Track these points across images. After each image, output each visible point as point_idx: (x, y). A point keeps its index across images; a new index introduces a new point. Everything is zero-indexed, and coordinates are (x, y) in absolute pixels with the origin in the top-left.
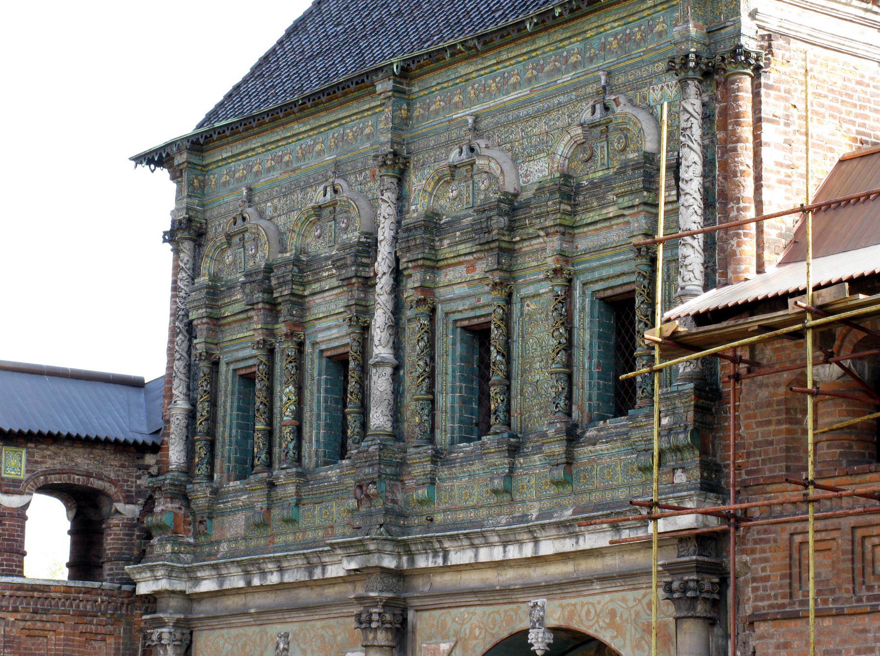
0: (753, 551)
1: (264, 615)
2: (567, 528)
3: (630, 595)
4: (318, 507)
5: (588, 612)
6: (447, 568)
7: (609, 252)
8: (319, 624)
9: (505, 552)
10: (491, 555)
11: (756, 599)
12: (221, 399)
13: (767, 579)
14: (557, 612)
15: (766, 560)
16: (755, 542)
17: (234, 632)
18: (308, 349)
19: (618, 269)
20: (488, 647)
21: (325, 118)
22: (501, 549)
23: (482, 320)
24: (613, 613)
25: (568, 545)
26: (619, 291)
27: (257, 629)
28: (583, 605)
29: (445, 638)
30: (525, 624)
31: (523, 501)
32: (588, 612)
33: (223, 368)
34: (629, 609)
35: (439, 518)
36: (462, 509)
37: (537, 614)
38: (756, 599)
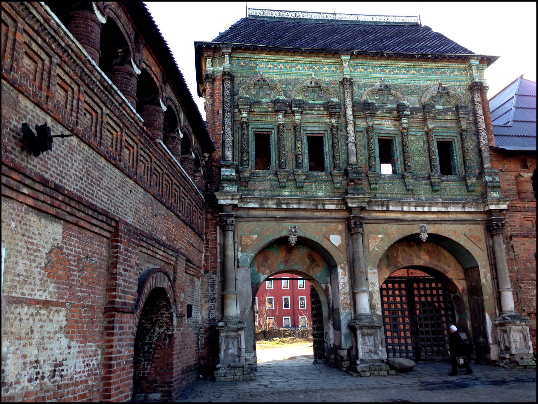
0: (509, 218)
3: (462, 226)
4: (314, 185)
5: (445, 230)
6: (388, 211)
7: (446, 129)
8: (312, 224)
9: (416, 209)
10: (409, 209)
11: (512, 231)
12: (250, 140)
13: (515, 226)
14: (432, 229)
15: (514, 221)
16: (510, 216)
17: (263, 224)
19: (449, 134)
20: (401, 237)
22: (414, 208)
23: (391, 138)
24: (455, 231)
25: (443, 209)
26: (445, 140)
27: (276, 224)
28: (442, 228)
30: (418, 231)
32: (445, 230)
33: (250, 129)
34: (461, 230)
35: (378, 195)
36: (390, 194)
38: (512, 231)
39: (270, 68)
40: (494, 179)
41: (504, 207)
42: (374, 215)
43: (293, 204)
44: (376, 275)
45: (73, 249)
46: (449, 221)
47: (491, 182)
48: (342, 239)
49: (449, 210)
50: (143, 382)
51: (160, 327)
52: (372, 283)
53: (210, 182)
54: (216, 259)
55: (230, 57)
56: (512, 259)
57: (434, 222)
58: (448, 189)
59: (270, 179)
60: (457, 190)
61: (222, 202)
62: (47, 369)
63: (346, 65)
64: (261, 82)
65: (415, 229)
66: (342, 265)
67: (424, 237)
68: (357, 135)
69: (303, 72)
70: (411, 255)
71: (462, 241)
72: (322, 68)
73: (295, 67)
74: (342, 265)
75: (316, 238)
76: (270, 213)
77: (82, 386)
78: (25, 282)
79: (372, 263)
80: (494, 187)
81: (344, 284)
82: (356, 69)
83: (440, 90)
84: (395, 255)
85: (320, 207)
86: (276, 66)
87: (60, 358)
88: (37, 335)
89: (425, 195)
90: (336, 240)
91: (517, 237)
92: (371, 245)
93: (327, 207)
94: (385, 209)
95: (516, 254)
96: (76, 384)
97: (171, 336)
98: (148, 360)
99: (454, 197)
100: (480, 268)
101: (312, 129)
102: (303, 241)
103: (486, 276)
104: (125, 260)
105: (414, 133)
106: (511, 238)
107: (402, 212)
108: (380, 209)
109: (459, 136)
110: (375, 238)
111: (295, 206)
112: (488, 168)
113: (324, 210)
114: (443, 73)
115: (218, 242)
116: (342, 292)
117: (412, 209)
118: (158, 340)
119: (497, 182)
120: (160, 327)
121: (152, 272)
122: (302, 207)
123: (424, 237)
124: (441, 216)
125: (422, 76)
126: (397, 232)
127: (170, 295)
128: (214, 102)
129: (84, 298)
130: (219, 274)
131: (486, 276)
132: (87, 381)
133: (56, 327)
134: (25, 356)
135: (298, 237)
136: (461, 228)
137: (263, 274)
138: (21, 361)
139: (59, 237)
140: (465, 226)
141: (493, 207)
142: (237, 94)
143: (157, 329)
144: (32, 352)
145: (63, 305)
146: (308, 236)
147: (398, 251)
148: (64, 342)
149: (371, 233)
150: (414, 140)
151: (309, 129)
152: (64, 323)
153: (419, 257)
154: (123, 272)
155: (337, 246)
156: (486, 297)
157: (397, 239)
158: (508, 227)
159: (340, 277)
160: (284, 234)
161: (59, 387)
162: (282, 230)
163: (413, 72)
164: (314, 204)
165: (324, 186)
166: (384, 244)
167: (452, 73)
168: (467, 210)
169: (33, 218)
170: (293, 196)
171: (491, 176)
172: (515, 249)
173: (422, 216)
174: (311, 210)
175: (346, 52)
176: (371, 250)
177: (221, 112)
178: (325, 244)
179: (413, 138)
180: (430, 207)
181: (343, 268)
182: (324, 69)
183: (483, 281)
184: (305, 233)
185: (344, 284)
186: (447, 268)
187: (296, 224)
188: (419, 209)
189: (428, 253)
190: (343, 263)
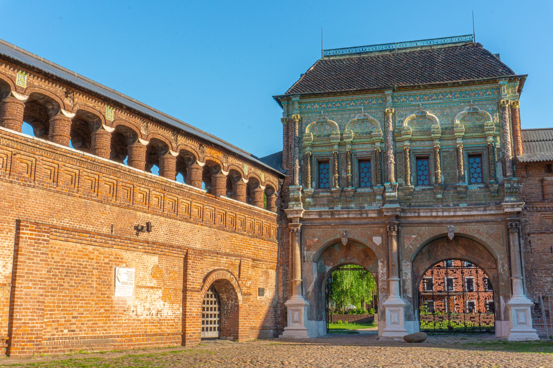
1: (337, 225)
2: (468, 209)
4: (361, 198)
5: (469, 230)
14: (458, 229)
18: (353, 157)
21: (361, 96)
24: (479, 230)
25: (466, 213)
29: (414, 235)
31: (447, 202)
32: (469, 230)
33: (313, 158)
37: (450, 229)
39: (330, 107)
40: (512, 186)
41: (519, 209)
42: (410, 219)
43: (344, 214)
44: (410, 267)
45: (164, 265)
46: (473, 222)
47: (509, 188)
48: (382, 239)
49: (472, 213)
50: (224, 330)
51: (232, 301)
52: (405, 273)
53: (283, 202)
54: (289, 256)
55: (300, 103)
56: (528, 252)
57: (460, 223)
58: (474, 195)
59: (327, 196)
60: (482, 196)
61: (290, 216)
62: (154, 312)
63: (389, 98)
64: (322, 120)
65: (442, 230)
66: (382, 259)
67: (451, 236)
68: (397, 156)
69: (355, 108)
70: (449, 250)
71: (483, 238)
72: (371, 102)
73: (349, 104)
74: (382, 259)
75: (362, 240)
76: (327, 221)
77: (172, 321)
78: (143, 280)
79: (406, 257)
80: (512, 193)
81: (383, 274)
82: (399, 100)
83: (471, 111)
84: (435, 249)
85: (364, 215)
86: (334, 105)
87: (160, 309)
88: (149, 299)
89: (453, 201)
90: (378, 240)
91: (534, 233)
92: (406, 244)
93: (370, 215)
94: (417, 215)
95: (532, 247)
96: (169, 320)
97: (238, 306)
98: (227, 319)
99: (479, 202)
100: (499, 260)
101: (362, 153)
102: (352, 243)
103: (503, 266)
104: (192, 267)
105: (446, 150)
106: (529, 235)
107: (431, 216)
108: (413, 215)
109: (487, 149)
110: (410, 238)
111: (345, 216)
112: (509, 176)
113: (367, 218)
114: (477, 94)
115: (290, 244)
116: (381, 280)
117: (440, 214)
118: (231, 308)
119: (515, 188)
120: (232, 301)
121: (214, 271)
122: (351, 216)
123: (451, 236)
124: (467, 218)
125: (457, 100)
126: (428, 233)
127: (234, 282)
128: (288, 139)
129: (171, 285)
130: (290, 267)
131: (503, 266)
132: (174, 320)
133: (157, 296)
134: (144, 306)
135: (349, 240)
136: (484, 228)
137: (328, 265)
138: (143, 308)
139: (157, 262)
140: (488, 226)
141: (507, 210)
142: (304, 132)
143: (230, 301)
144: (147, 305)
145: (160, 288)
146: (356, 238)
147: (438, 246)
148: (162, 303)
149: (407, 234)
150: (447, 155)
151: (358, 154)
152: (161, 295)
153: (456, 251)
154: (191, 273)
155: (378, 245)
156: (502, 284)
157: (428, 238)
158: (527, 225)
159: (380, 268)
160: (338, 236)
161: (160, 320)
162: (336, 234)
163: (449, 96)
164: (359, 214)
165: (368, 199)
166: (417, 242)
167: (485, 93)
168: (488, 212)
169: (145, 256)
170: (345, 208)
171: (510, 183)
172: (532, 244)
173: (449, 219)
174: (359, 218)
175: (389, 88)
176: (406, 247)
177: (293, 146)
178: (369, 244)
179: (445, 154)
180: (455, 212)
181: (382, 262)
182: (373, 103)
183: (501, 270)
184: (354, 236)
185: (383, 274)
186: (480, 260)
187: (347, 229)
188: (446, 214)
189: (464, 247)
190: (382, 258)
